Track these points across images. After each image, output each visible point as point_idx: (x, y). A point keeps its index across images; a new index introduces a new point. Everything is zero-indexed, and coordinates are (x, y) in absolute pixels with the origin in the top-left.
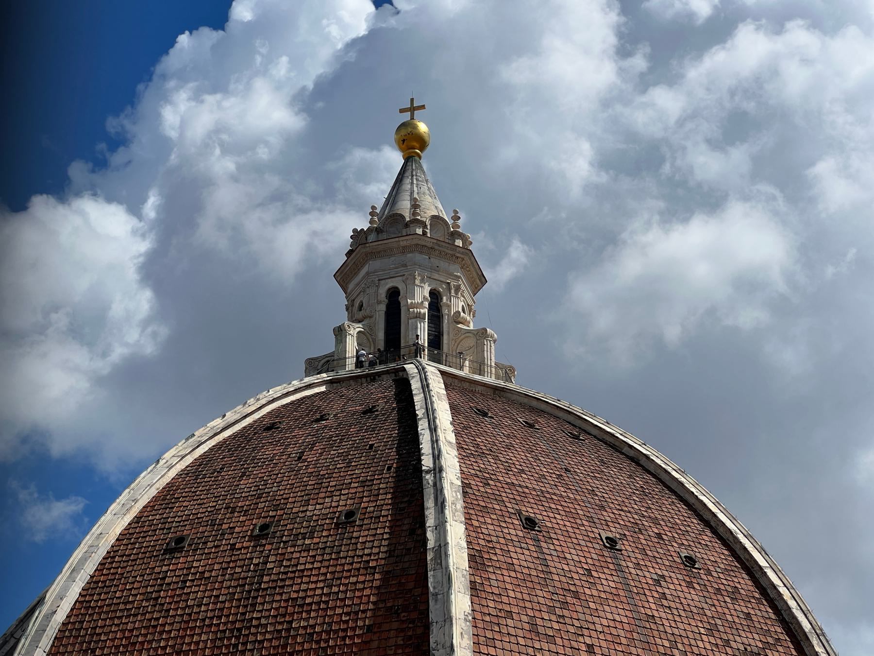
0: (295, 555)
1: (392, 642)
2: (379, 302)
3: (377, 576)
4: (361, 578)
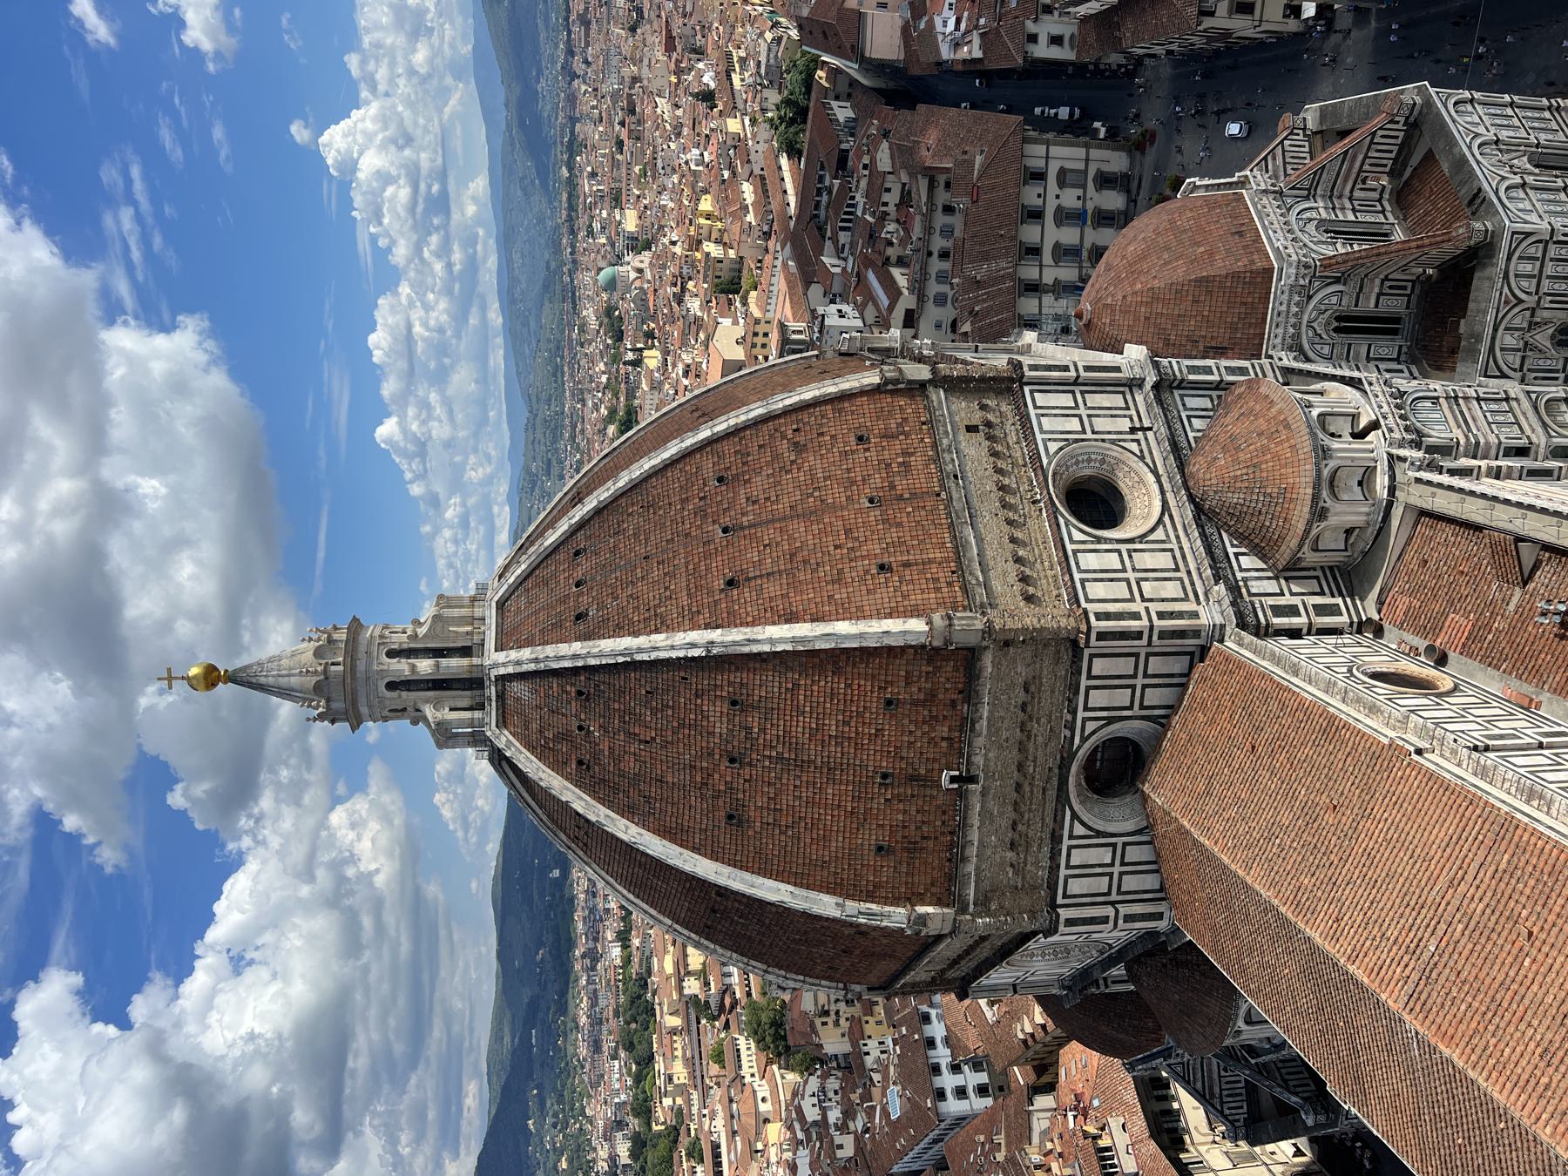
0: (768, 737)
1: (862, 671)
2: (400, 696)
3: (802, 682)
4: (802, 692)
